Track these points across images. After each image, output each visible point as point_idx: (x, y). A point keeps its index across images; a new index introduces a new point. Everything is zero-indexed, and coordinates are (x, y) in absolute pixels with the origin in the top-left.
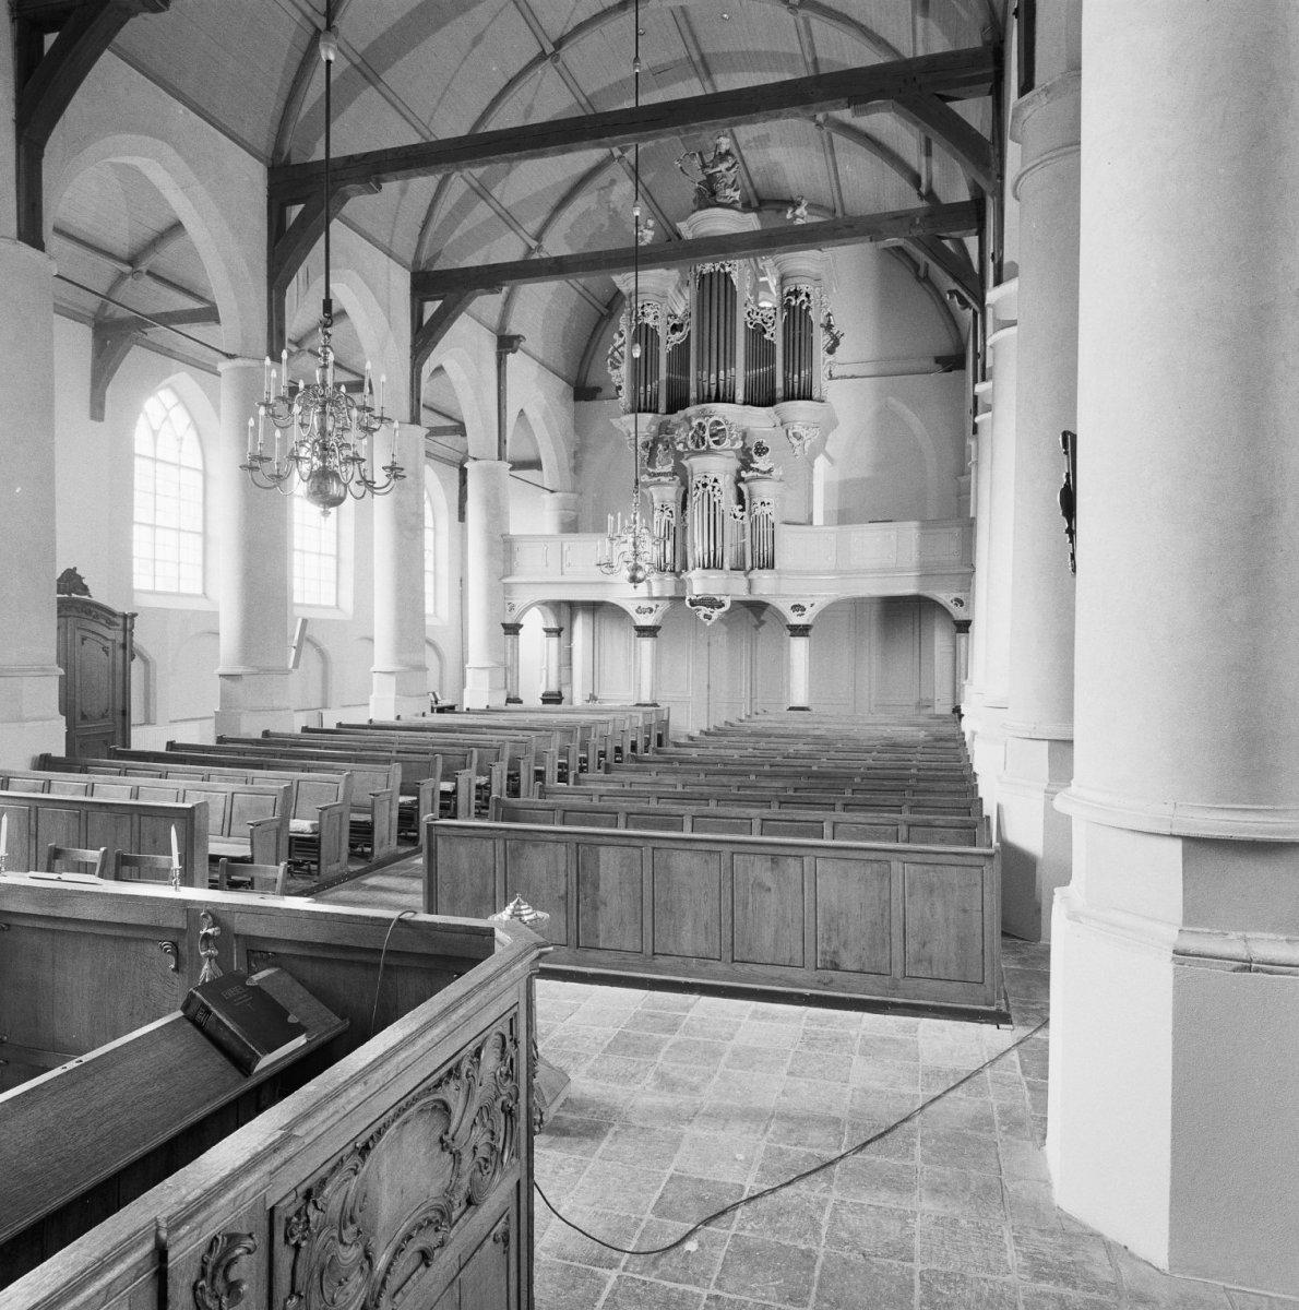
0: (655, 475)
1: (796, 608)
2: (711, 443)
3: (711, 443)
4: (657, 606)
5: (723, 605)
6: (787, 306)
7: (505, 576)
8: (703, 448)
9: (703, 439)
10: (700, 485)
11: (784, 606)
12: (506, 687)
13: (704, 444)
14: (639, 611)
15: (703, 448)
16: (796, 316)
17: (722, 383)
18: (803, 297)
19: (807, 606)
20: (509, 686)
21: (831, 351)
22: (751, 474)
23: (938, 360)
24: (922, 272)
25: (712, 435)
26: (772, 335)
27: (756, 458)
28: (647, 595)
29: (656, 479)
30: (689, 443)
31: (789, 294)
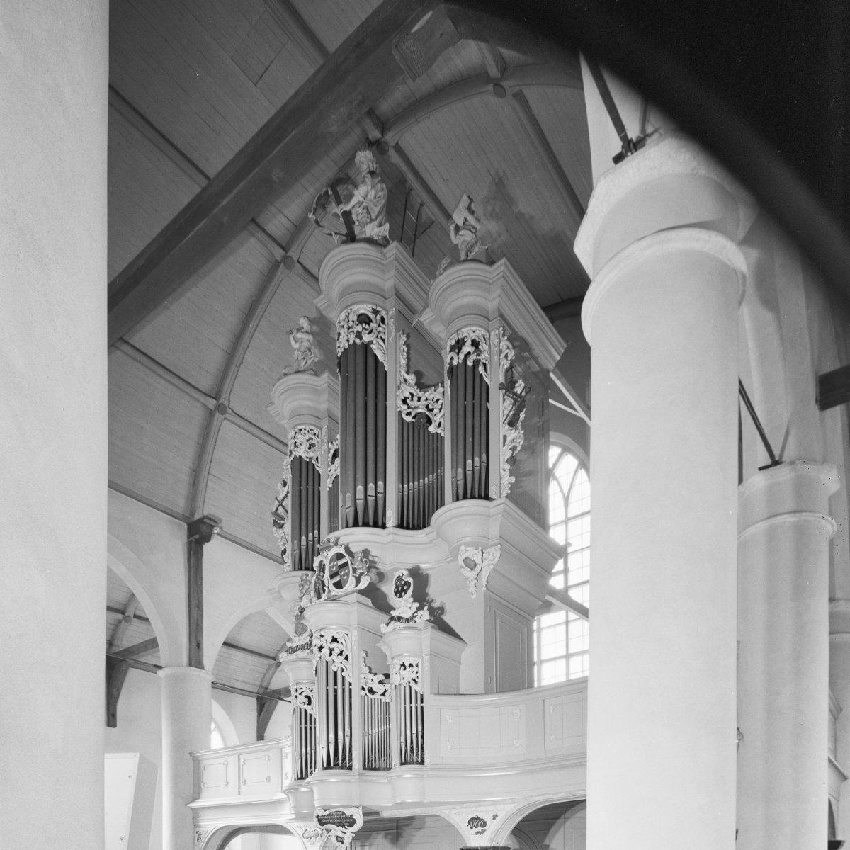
1: (476, 822)
2: (332, 587)
7: (194, 800)
11: (459, 819)
17: (371, 499)
19: (488, 818)
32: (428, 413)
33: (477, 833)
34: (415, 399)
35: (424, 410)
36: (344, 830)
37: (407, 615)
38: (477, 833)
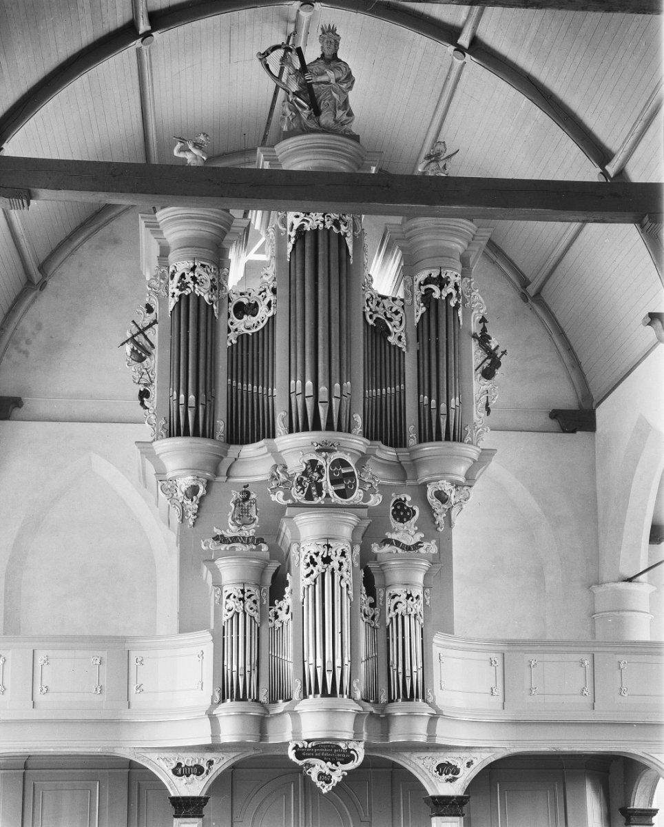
1: (443, 768)
5: (351, 758)
6: (427, 298)
8: (317, 501)
9: (319, 488)
10: (318, 560)
13: (320, 494)
14: (179, 771)
15: (317, 501)
16: (437, 318)
18: (450, 289)
19: (461, 765)
21: (488, 374)
23: (555, 414)
24: (532, 290)
26: (400, 338)
28: (208, 741)
29: (228, 547)
31: (429, 280)
32: (387, 322)
33: (447, 780)
34: (375, 303)
35: (383, 318)
36: (334, 767)
37: (411, 542)
38: (447, 780)
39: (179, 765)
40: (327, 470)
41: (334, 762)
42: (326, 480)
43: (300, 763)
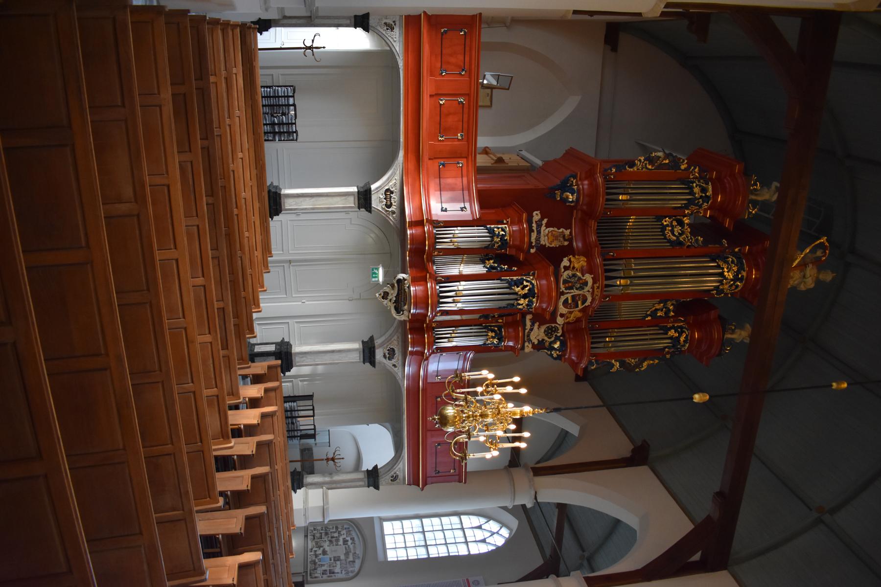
0: (539, 226)
3: (566, 296)
4: (393, 213)
8: (562, 288)
9: (571, 288)
12: (285, 17)
15: (562, 288)
19: (393, 361)
20: (285, 21)
22: (528, 323)
25: (573, 297)
27: (543, 328)
30: (569, 272)
39: (392, 192)
40: (581, 292)
41: (395, 302)
42: (575, 292)
43: (395, 282)
